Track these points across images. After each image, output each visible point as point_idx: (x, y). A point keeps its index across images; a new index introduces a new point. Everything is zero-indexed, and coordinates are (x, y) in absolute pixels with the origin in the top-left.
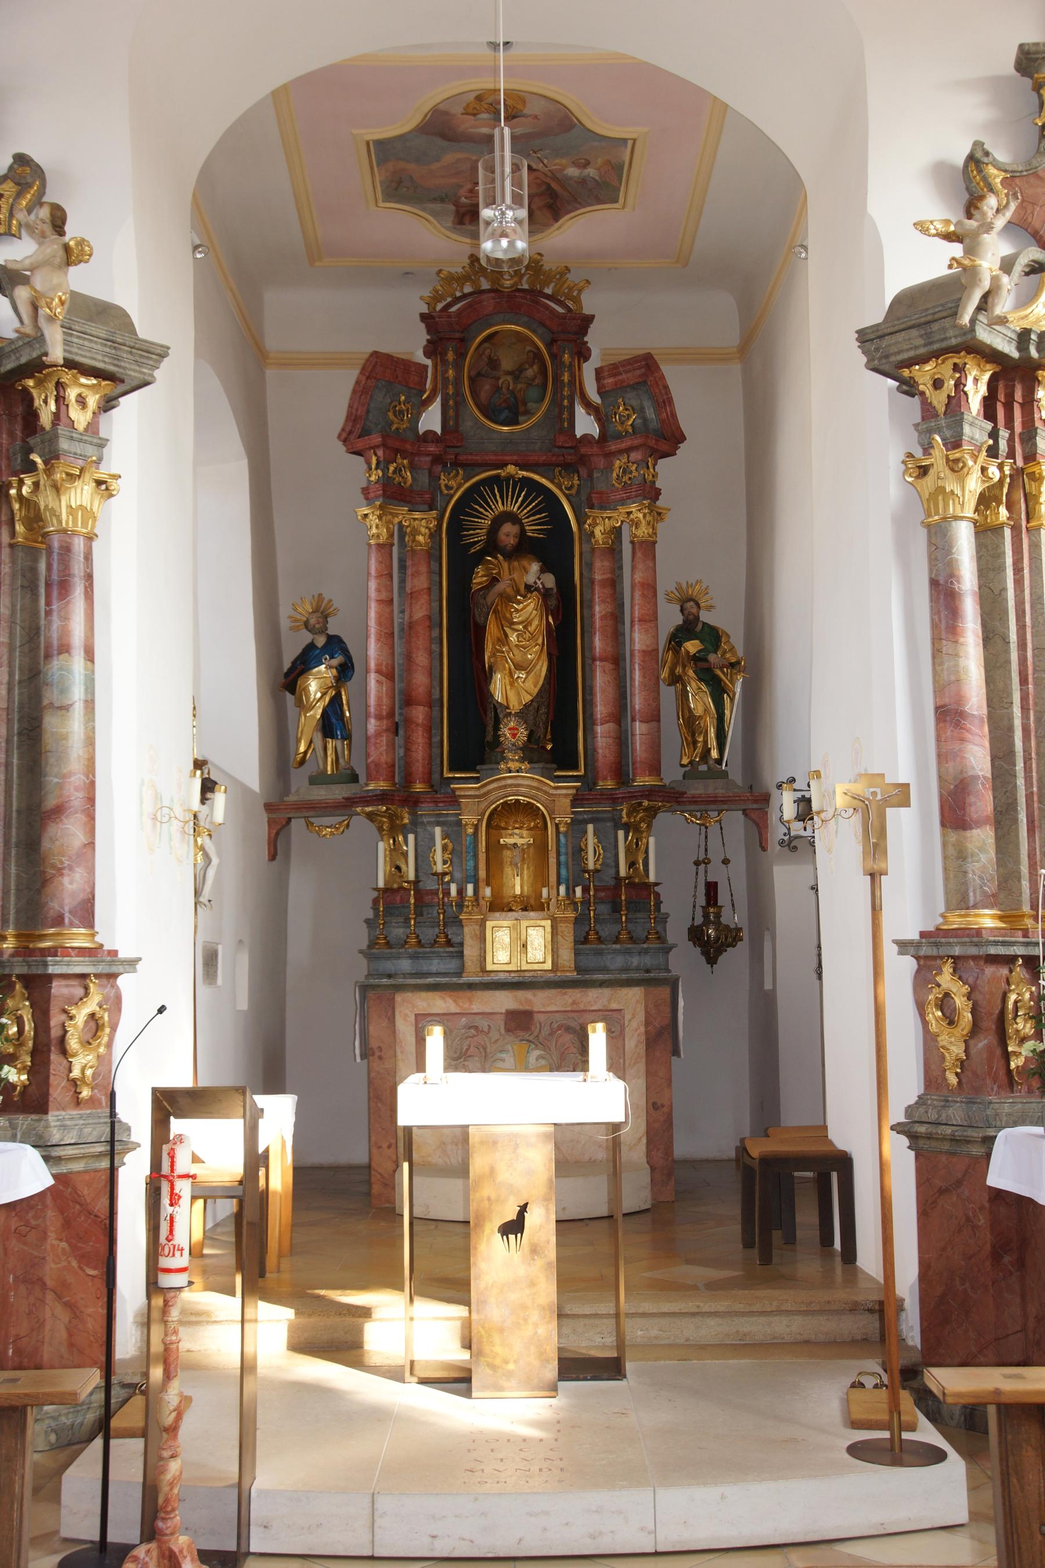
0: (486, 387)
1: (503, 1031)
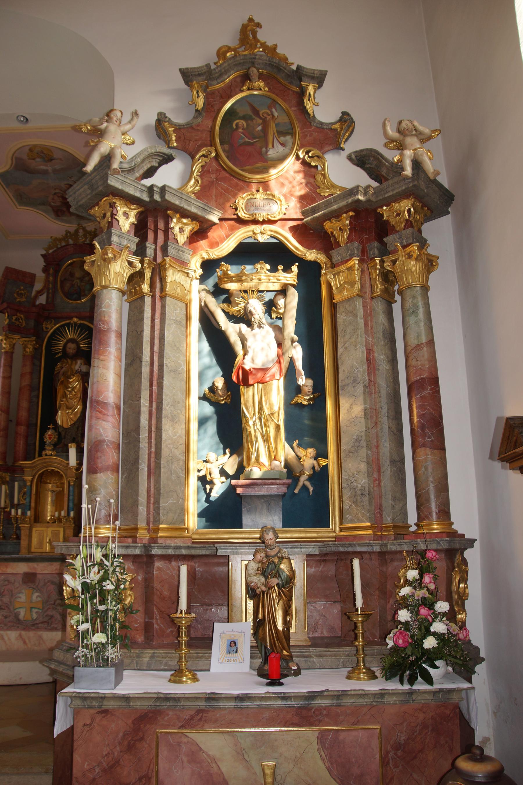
0: (68, 285)
1: (21, 582)
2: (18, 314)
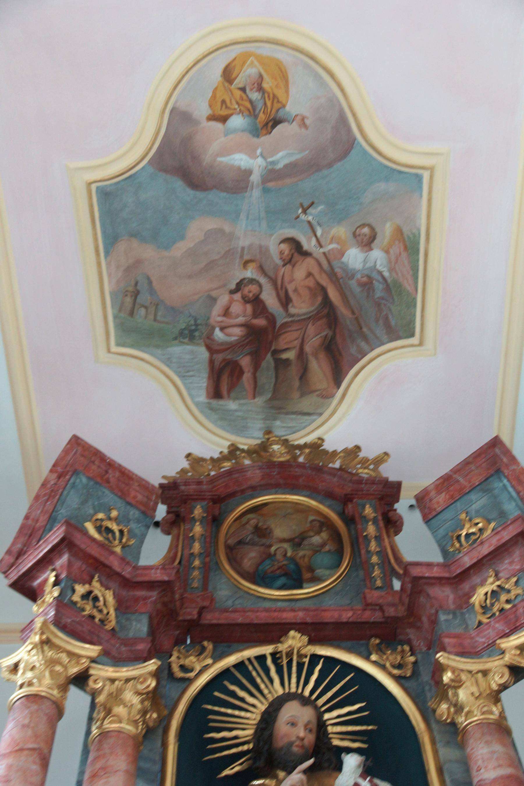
0: (250, 557)
2: (96, 584)
